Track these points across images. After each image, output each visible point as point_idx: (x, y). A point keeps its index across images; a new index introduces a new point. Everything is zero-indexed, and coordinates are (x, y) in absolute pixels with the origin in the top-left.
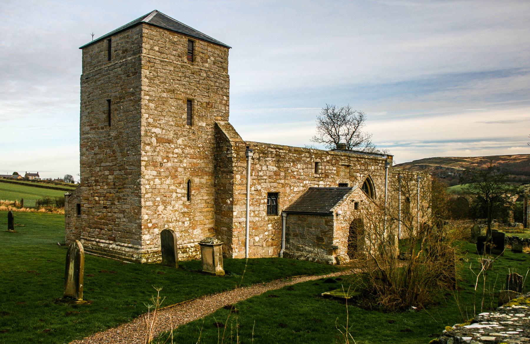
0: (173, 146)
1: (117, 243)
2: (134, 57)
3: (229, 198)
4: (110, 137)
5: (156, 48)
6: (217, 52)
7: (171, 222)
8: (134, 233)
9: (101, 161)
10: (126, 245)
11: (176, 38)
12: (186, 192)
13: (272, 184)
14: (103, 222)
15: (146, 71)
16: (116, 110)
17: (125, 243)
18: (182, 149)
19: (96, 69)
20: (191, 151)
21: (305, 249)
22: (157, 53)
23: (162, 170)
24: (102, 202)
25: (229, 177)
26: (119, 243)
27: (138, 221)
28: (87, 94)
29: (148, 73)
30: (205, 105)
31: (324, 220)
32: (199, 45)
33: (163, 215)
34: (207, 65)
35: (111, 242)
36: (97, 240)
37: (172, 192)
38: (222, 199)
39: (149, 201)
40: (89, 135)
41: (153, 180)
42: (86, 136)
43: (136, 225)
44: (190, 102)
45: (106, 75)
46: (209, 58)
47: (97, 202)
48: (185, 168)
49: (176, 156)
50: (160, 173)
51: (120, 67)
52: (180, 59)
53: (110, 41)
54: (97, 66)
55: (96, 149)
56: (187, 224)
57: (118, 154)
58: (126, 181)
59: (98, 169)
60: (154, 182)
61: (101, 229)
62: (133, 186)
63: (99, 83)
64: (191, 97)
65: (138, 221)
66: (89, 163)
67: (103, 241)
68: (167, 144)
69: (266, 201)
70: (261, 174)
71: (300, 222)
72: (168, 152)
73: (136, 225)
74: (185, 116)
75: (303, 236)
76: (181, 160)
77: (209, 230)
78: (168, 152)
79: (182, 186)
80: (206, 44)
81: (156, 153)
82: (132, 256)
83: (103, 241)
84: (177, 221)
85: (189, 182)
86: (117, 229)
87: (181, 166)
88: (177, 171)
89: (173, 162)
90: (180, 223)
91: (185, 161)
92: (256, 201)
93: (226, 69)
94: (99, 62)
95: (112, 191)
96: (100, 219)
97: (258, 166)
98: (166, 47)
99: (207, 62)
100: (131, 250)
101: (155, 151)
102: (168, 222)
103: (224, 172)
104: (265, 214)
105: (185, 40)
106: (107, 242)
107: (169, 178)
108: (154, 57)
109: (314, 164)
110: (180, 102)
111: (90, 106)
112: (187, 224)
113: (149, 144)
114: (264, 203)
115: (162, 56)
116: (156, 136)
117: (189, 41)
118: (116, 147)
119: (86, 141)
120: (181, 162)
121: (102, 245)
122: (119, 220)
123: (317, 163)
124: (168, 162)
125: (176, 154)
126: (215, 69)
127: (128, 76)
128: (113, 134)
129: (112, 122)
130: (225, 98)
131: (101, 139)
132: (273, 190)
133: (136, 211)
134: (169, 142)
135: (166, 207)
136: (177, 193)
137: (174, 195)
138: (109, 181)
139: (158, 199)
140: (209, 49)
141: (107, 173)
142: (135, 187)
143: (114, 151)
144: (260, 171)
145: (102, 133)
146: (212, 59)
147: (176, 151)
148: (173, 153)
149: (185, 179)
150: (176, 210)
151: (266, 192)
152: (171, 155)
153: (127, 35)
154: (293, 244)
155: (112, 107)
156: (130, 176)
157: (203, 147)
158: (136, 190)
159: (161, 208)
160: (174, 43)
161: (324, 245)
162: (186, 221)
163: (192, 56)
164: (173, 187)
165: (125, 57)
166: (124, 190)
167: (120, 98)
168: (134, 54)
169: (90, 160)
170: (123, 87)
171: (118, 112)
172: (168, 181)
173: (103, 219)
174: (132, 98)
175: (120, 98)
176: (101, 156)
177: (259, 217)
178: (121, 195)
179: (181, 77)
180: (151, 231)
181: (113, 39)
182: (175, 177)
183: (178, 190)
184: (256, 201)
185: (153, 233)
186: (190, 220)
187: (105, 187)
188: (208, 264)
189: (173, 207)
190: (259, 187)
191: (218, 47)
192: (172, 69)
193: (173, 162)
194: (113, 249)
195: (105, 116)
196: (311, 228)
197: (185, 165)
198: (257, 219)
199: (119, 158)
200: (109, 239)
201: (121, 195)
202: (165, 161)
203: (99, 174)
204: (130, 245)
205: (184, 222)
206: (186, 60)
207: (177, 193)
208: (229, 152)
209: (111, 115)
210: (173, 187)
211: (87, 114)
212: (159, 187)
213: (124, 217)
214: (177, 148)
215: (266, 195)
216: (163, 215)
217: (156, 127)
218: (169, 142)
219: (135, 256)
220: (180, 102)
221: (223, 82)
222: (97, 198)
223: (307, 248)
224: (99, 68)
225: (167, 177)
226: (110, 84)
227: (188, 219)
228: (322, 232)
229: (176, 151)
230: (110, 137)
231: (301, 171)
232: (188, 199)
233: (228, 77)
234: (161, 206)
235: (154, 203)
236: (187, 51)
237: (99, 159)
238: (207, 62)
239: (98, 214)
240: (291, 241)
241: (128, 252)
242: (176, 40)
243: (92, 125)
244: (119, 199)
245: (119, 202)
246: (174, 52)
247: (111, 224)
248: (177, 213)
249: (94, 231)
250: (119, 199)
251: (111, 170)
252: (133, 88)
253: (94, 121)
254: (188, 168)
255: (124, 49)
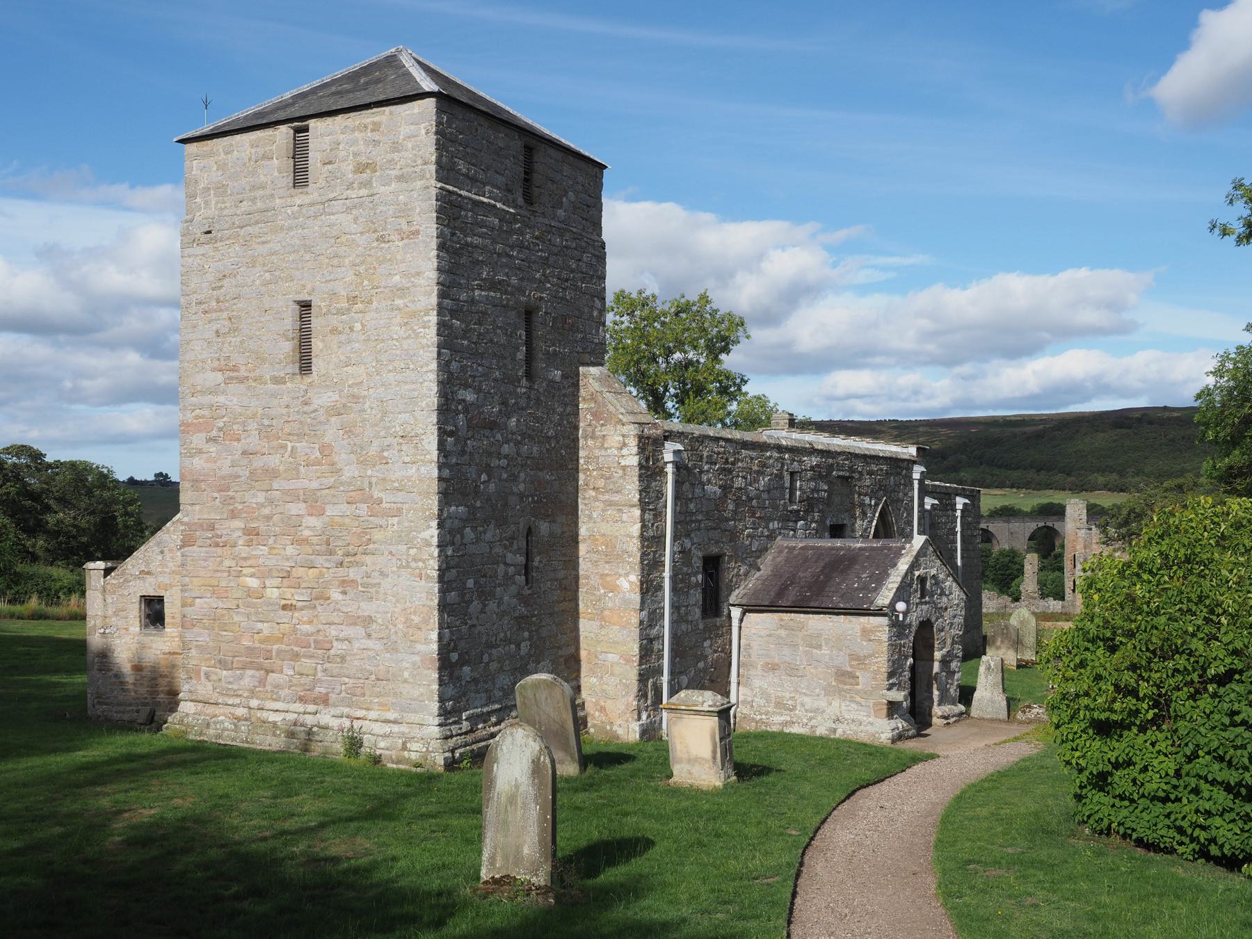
0: (499, 437)
1: (338, 711)
2: (404, 185)
3: (627, 575)
4: (311, 408)
6: (580, 179)
7: (493, 647)
8: (406, 681)
9: (273, 474)
10: (373, 715)
11: (501, 138)
12: (521, 559)
13: (712, 534)
14: (279, 652)
16: (334, 331)
17: (368, 709)
18: (518, 443)
19: (245, 206)
20: (535, 449)
21: (803, 705)
23: (478, 504)
24: (272, 593)
25: (625, 517)
26: (346, 710)
27: (420, 647)
28: (210, 277)
31: (858, 628)
32: (543, 160)
33: (479, 628)
34: (561, 213)
35: (311, 708)
36: (254, 703)
37: (498, 563)
38: (603, 576)
39: (453, 590)
40: (221, 399)
41: (460, 531)
42: (207, 399)
43: (417, 658)
45: (290, 229)
47: (249, 592)
48: (521, 496)
49: (504, 462)
50: (472, 510)
51: (348, 210)
53: (306, 129)
54: (254, 200)
55: (253, 441)
56: (525, 647)
57: (342, 458)
58: (377, 535)
59: (261, 497)
60: (462, 537)
61: (268, 672)
62: (403, 548)
63: (261, 249)
65: (420, 647)
66: (223, 478)
67: (279, 705)
68: (487, 432)
69: (700, 577)
70: (692, 506)
71: (783, 633)
72: (490, 454)
73: (417, 658)
74: (521, 355)
75: (792, 670)
76: (513, 475)
77: (566, 661)
78: (490, 454)
79: (515, 547)
80: (559, 155)
81: (467, 457)
82: (404, 748)
83: (279, 705)
84: (508, 641)
85: (530, 532)
86: (335, 672)
87: (515, 489)
88: (506, 505)
89: (500, 480)
90: (513, 646)
91: (522, 475)
92: (682, 581)
94: (253, 188)
95: (320, 560)
96: (266, 640)
97: (686, 486)
100: (396, 728)
101: (463, 452)
102: (490, 646)
103: (611, 504)
104: (697, 612)
105: (517, 144)
106: (299, 707)
107: (492, 526)
109: (787, 478)
110: (513, 314)
111: (225, 315)
112: (525, 647)
113: (451, 434)
114: (697, 585)
116: (466, 411)
117: (526, 147)
118: (331, 433)
119: (206, 412)
120: (514, 478)
121: (273, 717)
122: (345, 646)
123: (792, 474)
124: (489, 481)
125: (506, 457)
127: (381, 239)
128: (324, 399)
129: (318, 364)
130: (598, 303)
131: (273, 412)
132: (714, 550)
133: (416, 619)
134: (492, 426)
135: (485, 606)
136: (505, 564)
137: (501, 569)
138: (307, 533)
139: (470, 583)
140: (567, 170)
141: (296, 508)
142: (413, 552)
143: (326, 450)
144: (691, 500)
145: (274, 395)
147: (506, 449)
148: (499, 456)
149: (521, 526)
150: (504, 613)
151: (700, 554)
152: (495, 462)
153: (374, 123)
154: (765, 694)
155: (316, 323)
156: (396, 519)
157: (556, 437)
158: (415, 560)
159: (475, 606)
161: (858, 692)
162: (524, 640)
164: (498, 550)
165: (363, 185)
166: (368, 559)
167: (353, 300)
168: (400, 178)
169: (226, 470)
170: (362, 269)
171: (343, 338)
172: (488, 536)
173: (280, 640)
174: (399, 302)
175: (353, 300)
176: (274, 461)
177: (687, 622)
178: (353, 573)
180: (457, 673)
181: (312, 123)
182: (502, 522)
183: (510, 557)
184: (682, 581)
185: (459, 679)
186: (530, 639)
187: (290, 550)
188: (693, 761)
189: (499, 605)
190: (688, 544)
191: (582, 165)
193: (500, 480)
194: (326, 728)
195: (287, 347)
196: (819, 647)
197: (522, 487)
198: (684, 627)
199: (349, 472)
200: (301, 699)
201: (353, 573)
202: (484, 477)
203: (266, 511)
204: (391, 715)
205: (518, 646)
206: (520, 201)
207: (505, 564)
208: (625, 451)
209: (317, 345)
210: (498, 550)
211: (210, 334)
212: (472, 549)
213: (369, 636)
214: (507, 442)
215: (698, 563)
216: (479, 628)
217: (466, 386)
218: (492, 426)
219: (414, 746)
220: (513, 314)
221: (594, 261)
222: (253, 583)
223: (806, 700)
224: (259, 205)
225: (486, 522)
226: (307, 257)
227: (526, 634)
228: (853, 657)
229: (506, 449)
230: (306, 408)
231: (765, 496)
232: (527, 583)
233: (603, 245)
234: (475, 603)
235: (462, 595)
236: (522, 175)
237: (266, 471)
239: (260, 625)
240: (757, 683)
241: (385, 736)
242: (501, 145)
243: (235, 369)
244: (345, 584)
245: (344, 593)
246: (500, 180)
247: (311, 657)
248: (506, 620)
249: (241, 677)
250: (345, 584)
251: (314, 503)
252: (404, 274)
253: (237, 359)
254: (528, 497)
255: (363, 159)
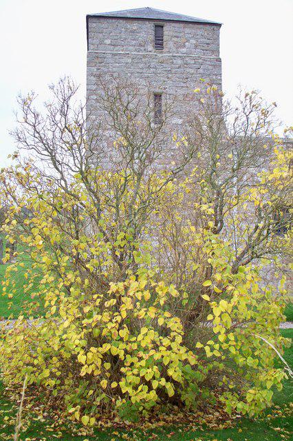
5: (108, 42)
15: (93, 68)
22: (109, 47)
29: (95, 70)
30: (181, 98)
34: (184, 50)
44: (158, 96)
46: (188, 41)
52: (142, 48)
64: (160, 91)
80: (182, 25)
93: (216, 51)
98: (121, 38)
99: (184, 46)
105: (150, 27)
108: (104, 52)
115: (117, 48)
117: (156, 26)
126: (197, 53)
146: (193, 41)
160: (133, 32)
163: (159, 43)
179: (142, 69)
192: (130, 61)
233: (220, 60)
238: (184, 46)
246: (134, 42)
